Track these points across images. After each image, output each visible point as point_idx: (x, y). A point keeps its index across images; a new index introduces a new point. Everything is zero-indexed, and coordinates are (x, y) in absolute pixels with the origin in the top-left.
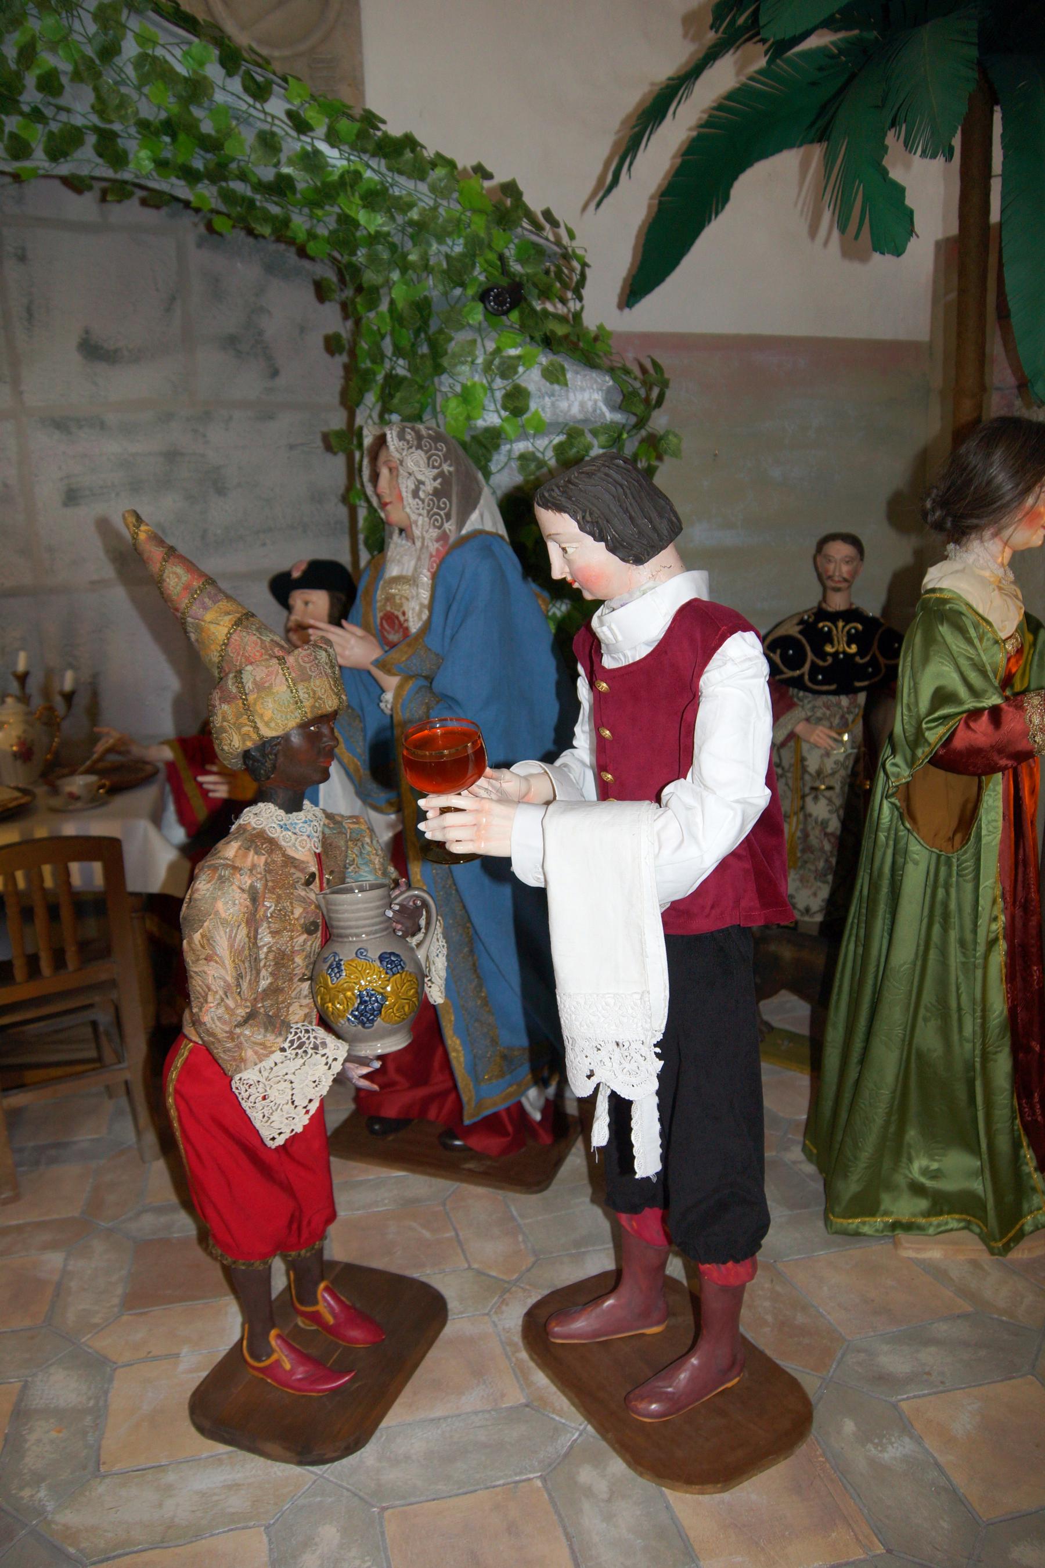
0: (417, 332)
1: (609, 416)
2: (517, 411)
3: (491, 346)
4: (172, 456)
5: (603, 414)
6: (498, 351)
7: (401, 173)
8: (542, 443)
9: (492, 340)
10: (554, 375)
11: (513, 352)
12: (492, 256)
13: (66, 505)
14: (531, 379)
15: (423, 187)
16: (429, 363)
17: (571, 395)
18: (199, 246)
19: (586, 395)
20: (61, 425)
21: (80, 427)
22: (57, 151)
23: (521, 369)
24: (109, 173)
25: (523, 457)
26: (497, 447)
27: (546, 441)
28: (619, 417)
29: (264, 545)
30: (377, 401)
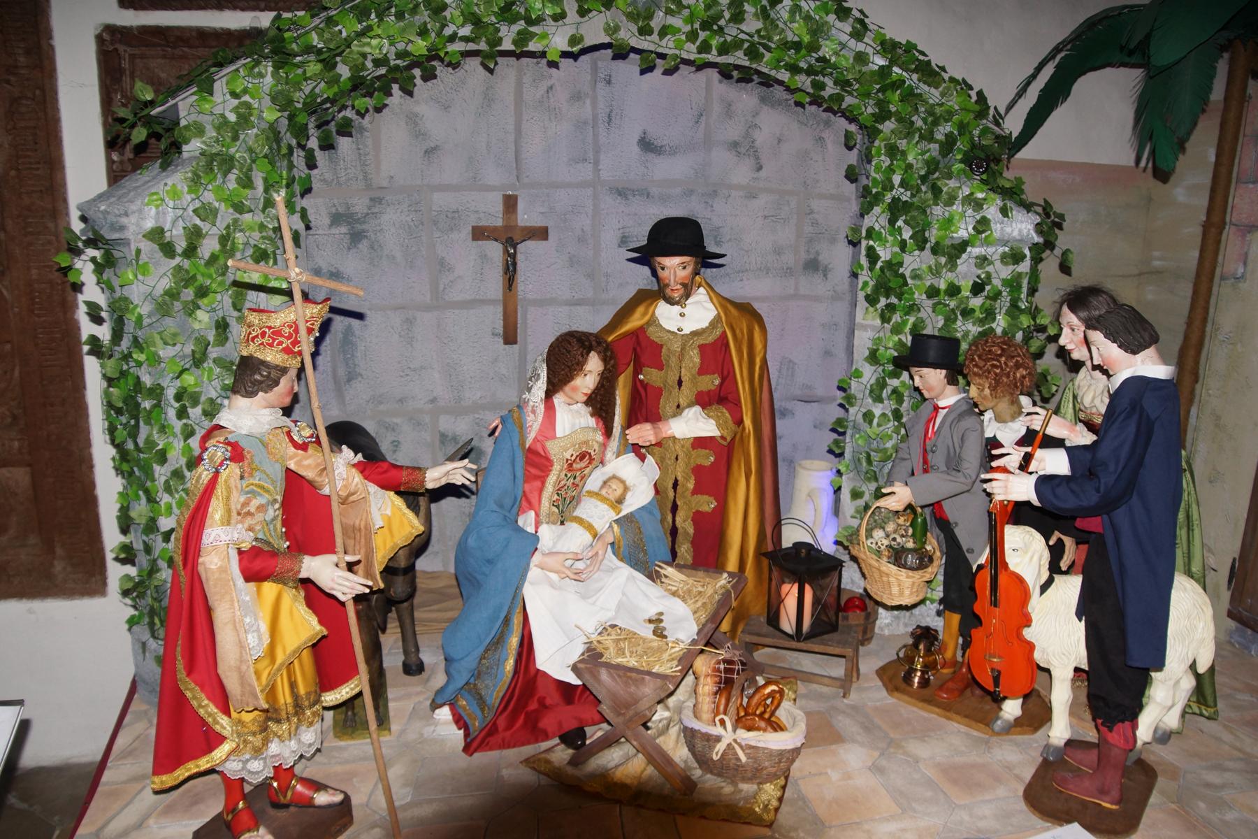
0: (924, 179)
1: (1037, 239)
2: (979, 232)
3: (967, 191)
5: (1033, 238)
6: (972, 194)
7: (925, 83)
8: (991, 250)
9: (968, 186)
10: (1004, 212)
11: (980, 195)
12: (968, 136)
13: (620, 246)
14: (992, 212)
15: (933, 90)
16: (929, 195)
17: (1014, 224)
19: (1024, 226)
20: (622, 193)
21: (634, 196)
22: (724, 50)
23: (985, 207)
24: (747, 64)
25: (977, 257)
26: (965, 251)
27: (994, 249)
28: (1041, 240)
30: (883, 212)
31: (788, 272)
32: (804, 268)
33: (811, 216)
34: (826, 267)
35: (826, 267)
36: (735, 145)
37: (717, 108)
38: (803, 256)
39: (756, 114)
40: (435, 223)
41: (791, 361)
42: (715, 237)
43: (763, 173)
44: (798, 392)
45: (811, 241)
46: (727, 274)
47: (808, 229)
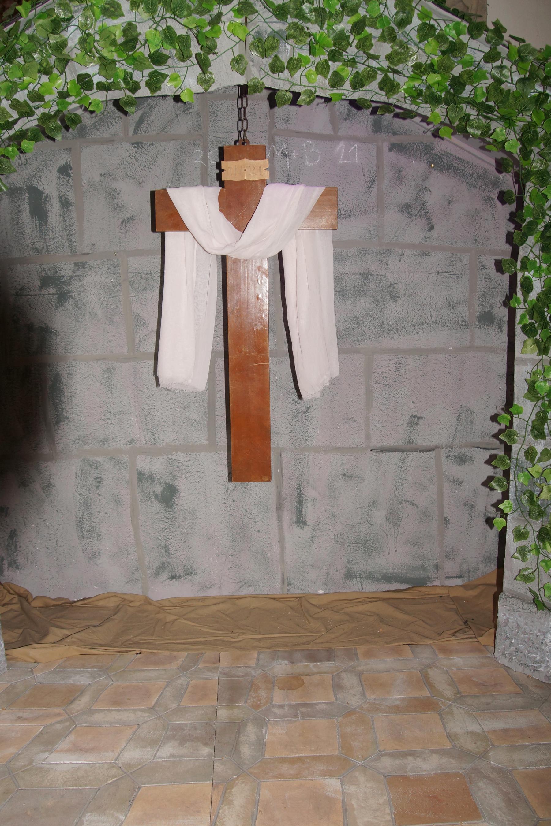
4: (366, 275)
18: (390, 150)
29: (417, 333)
31: (464, 325)
32: (479, 321)
33: (483, 272)
34: (501, 319)
35: (501, 319)
36: (406, 207)
37: (388, 173)
38: (478, 310)
39: (425, 178)
40: (131, 284)
41: (469, 410)
42: (391, 293)
43: (434, 233)
44: (477, 440)
45: (484, 295)
46: (404, 327)
47: (481, 284)
